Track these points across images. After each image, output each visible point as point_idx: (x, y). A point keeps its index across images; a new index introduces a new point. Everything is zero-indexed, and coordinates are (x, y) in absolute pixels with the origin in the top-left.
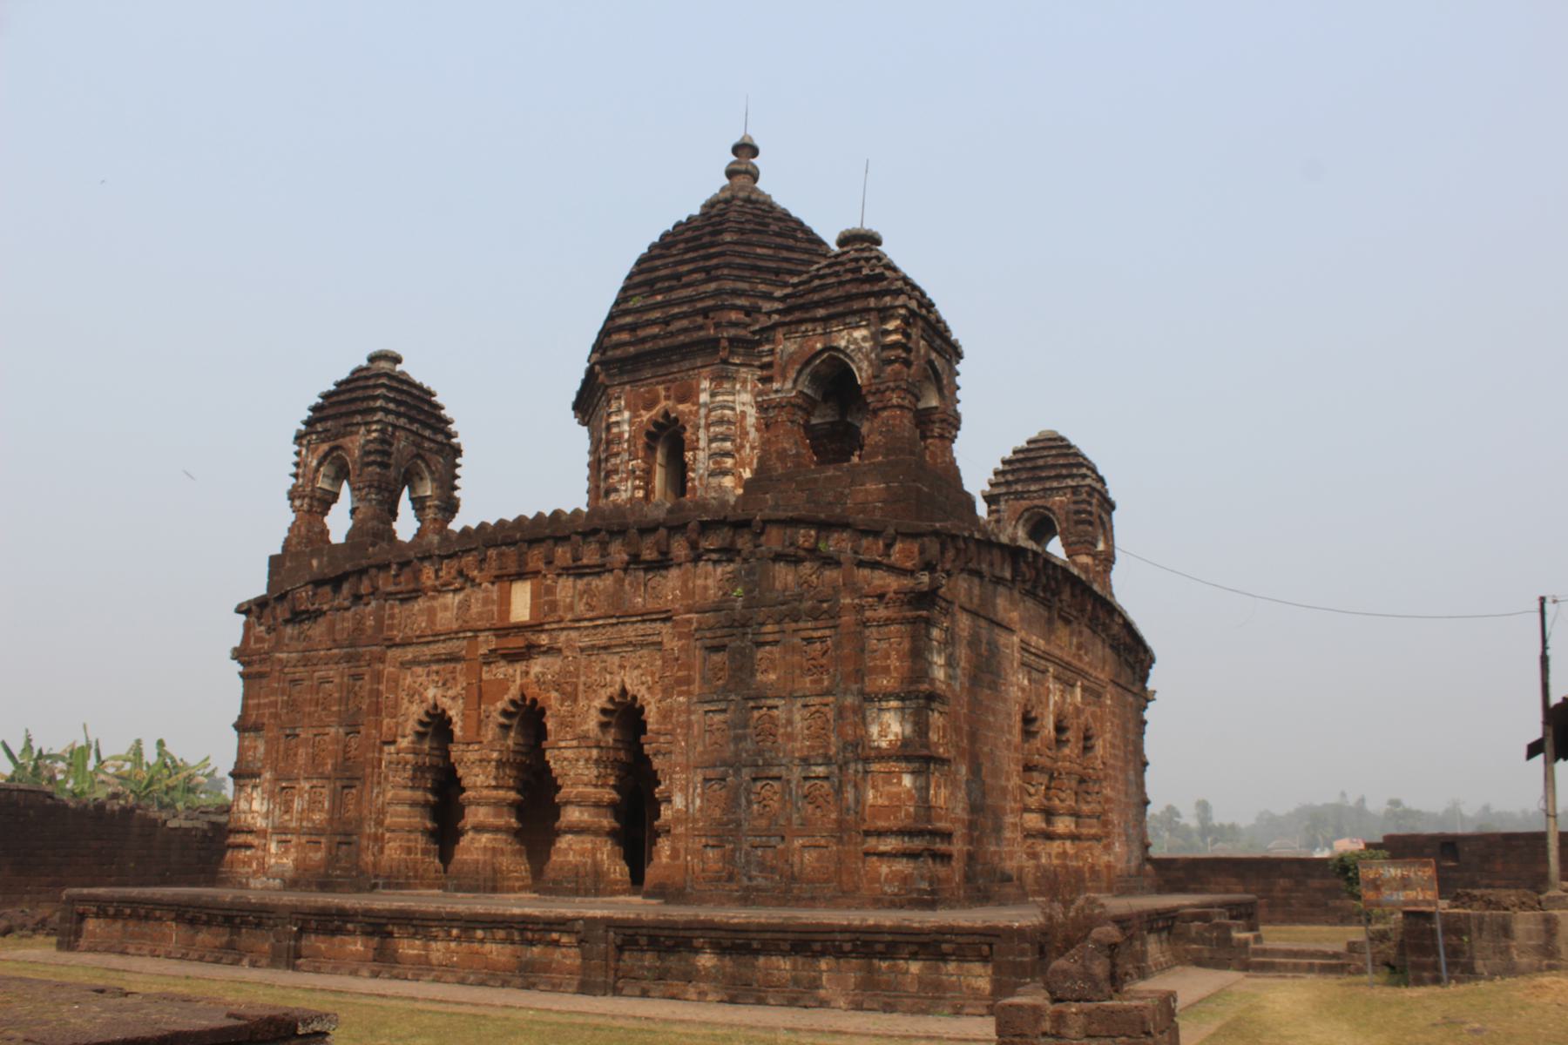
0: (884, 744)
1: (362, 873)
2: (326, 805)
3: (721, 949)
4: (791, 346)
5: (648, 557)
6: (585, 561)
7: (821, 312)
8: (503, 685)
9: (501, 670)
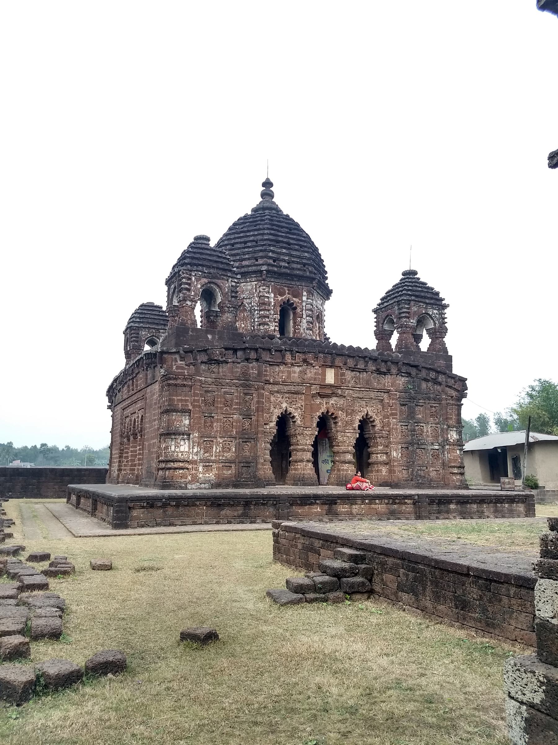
0: (452, 441)
1: (260, 479)
2: (234, 449)
3: (458, 503)
4: (414, 309)
5: (382, 370)
6: (358, 367)
7: (427, 301)
8: (319, 406)
9: (318, 401)
